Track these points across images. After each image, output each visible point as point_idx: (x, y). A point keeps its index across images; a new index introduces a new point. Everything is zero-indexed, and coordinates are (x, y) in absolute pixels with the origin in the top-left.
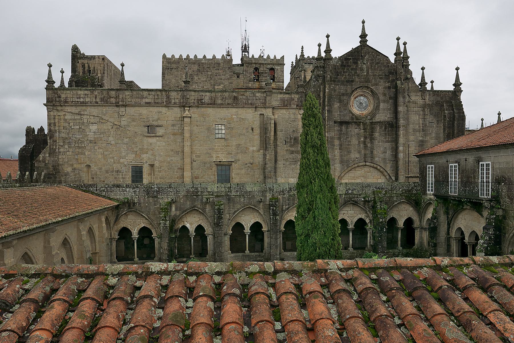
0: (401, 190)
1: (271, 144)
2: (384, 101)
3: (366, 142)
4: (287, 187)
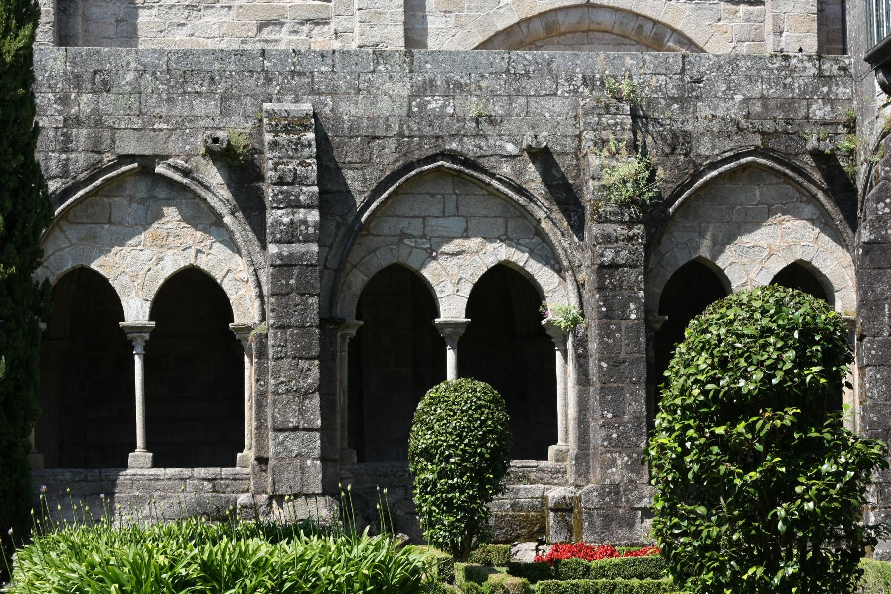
0: (739, 97)
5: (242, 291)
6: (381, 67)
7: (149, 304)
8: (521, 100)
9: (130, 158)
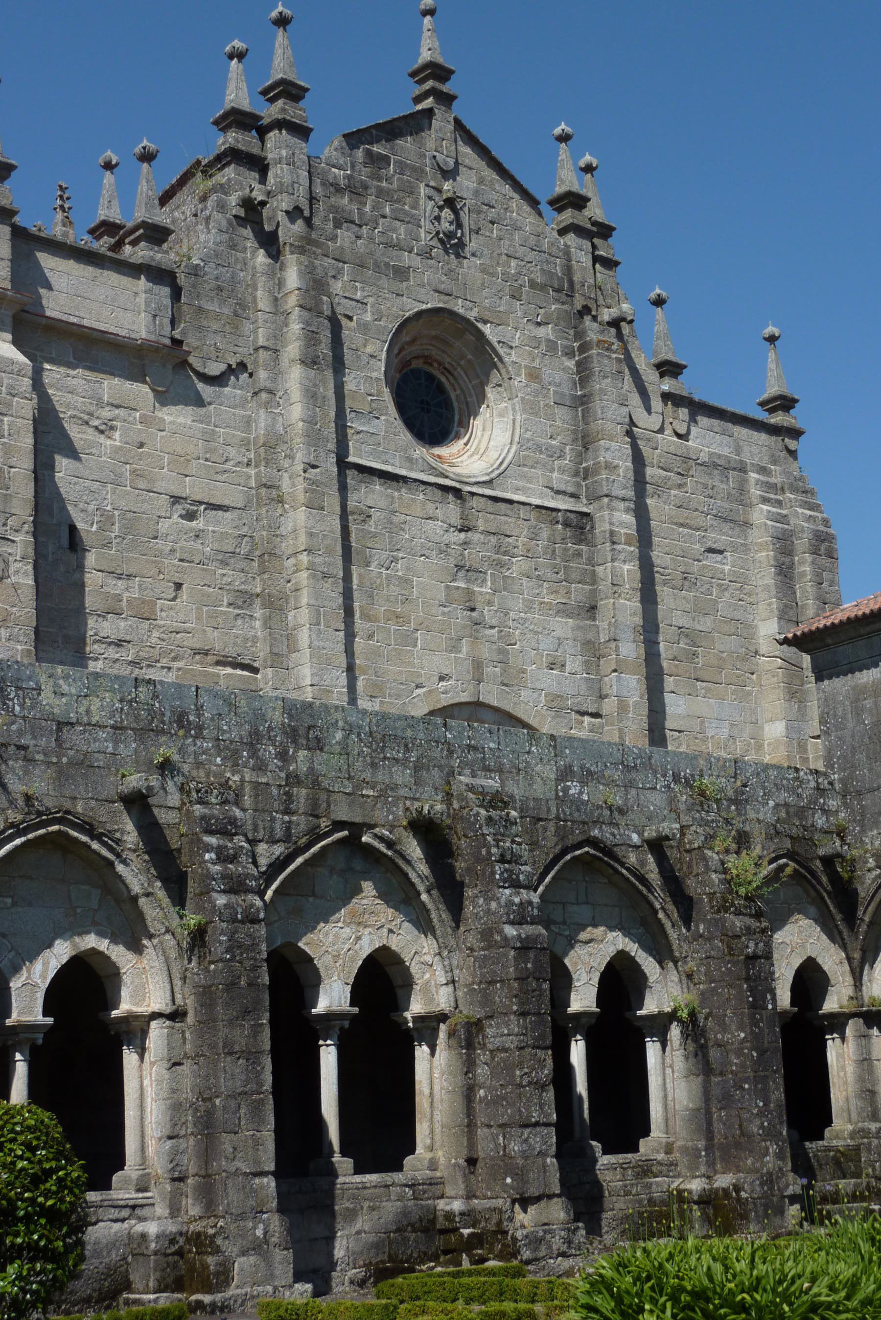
5: (427, 976)
6: (533, 749)
7: (348, 988)
8: (633, 792)
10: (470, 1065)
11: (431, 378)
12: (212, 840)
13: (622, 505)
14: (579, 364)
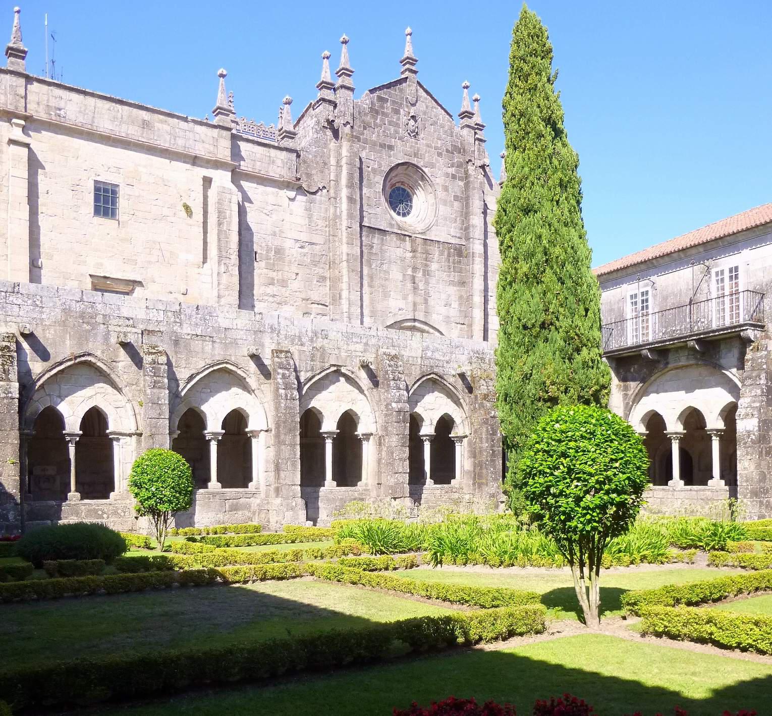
1: (231, 251)
2: (445, 203)
3: (417, 279)
4: (309, 330)
9: (334, 365)
10: (380, 452)
11: (404, 190)
12: (280, 371)
13: (477, 242)
14: (465, 184)
